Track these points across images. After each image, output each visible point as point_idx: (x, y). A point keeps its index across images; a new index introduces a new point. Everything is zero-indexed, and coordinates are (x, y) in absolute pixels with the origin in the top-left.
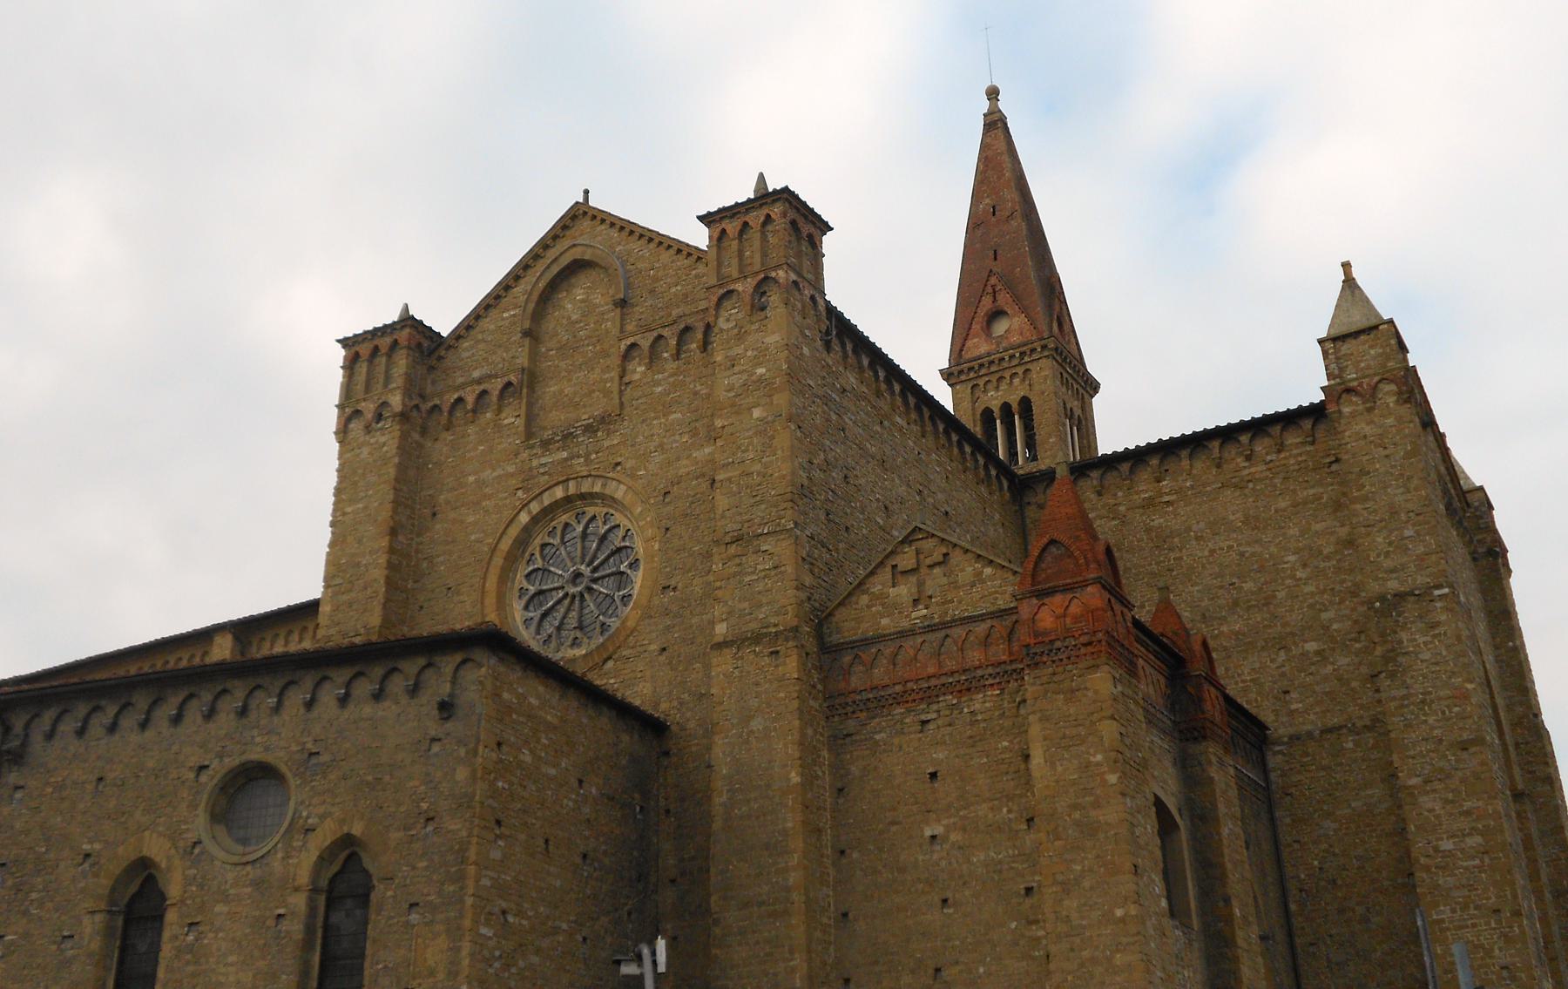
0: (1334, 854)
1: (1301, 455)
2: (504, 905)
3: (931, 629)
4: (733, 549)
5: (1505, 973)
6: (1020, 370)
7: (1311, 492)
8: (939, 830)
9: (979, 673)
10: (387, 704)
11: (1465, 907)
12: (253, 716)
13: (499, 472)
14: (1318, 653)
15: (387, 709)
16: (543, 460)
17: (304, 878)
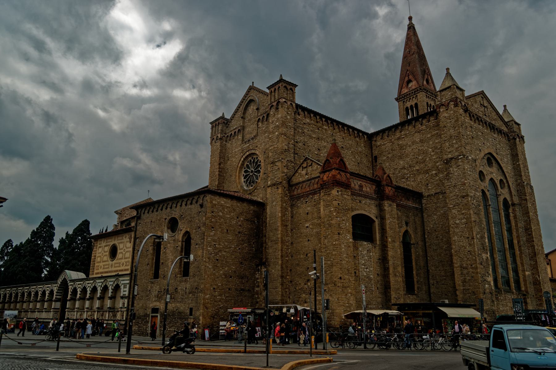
0: (436, 224)
1: (434, 122)
2: (215, 243)
3: (308, 180)
4: (272, 165)
5: (469, 253)
6: (415, 96)
7: (436, 132)
8: (308, 225)
9: (316, 190)
10: (193, 205)
11: (461, 237)
12: (173, 208)
13: (238, 149)
14: (436, 174)
15: (193, 206)
16: (245, 146)
17: (180, 239)
